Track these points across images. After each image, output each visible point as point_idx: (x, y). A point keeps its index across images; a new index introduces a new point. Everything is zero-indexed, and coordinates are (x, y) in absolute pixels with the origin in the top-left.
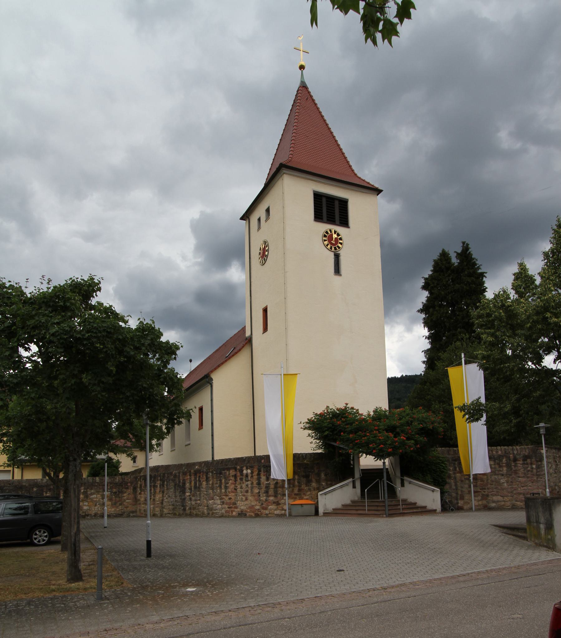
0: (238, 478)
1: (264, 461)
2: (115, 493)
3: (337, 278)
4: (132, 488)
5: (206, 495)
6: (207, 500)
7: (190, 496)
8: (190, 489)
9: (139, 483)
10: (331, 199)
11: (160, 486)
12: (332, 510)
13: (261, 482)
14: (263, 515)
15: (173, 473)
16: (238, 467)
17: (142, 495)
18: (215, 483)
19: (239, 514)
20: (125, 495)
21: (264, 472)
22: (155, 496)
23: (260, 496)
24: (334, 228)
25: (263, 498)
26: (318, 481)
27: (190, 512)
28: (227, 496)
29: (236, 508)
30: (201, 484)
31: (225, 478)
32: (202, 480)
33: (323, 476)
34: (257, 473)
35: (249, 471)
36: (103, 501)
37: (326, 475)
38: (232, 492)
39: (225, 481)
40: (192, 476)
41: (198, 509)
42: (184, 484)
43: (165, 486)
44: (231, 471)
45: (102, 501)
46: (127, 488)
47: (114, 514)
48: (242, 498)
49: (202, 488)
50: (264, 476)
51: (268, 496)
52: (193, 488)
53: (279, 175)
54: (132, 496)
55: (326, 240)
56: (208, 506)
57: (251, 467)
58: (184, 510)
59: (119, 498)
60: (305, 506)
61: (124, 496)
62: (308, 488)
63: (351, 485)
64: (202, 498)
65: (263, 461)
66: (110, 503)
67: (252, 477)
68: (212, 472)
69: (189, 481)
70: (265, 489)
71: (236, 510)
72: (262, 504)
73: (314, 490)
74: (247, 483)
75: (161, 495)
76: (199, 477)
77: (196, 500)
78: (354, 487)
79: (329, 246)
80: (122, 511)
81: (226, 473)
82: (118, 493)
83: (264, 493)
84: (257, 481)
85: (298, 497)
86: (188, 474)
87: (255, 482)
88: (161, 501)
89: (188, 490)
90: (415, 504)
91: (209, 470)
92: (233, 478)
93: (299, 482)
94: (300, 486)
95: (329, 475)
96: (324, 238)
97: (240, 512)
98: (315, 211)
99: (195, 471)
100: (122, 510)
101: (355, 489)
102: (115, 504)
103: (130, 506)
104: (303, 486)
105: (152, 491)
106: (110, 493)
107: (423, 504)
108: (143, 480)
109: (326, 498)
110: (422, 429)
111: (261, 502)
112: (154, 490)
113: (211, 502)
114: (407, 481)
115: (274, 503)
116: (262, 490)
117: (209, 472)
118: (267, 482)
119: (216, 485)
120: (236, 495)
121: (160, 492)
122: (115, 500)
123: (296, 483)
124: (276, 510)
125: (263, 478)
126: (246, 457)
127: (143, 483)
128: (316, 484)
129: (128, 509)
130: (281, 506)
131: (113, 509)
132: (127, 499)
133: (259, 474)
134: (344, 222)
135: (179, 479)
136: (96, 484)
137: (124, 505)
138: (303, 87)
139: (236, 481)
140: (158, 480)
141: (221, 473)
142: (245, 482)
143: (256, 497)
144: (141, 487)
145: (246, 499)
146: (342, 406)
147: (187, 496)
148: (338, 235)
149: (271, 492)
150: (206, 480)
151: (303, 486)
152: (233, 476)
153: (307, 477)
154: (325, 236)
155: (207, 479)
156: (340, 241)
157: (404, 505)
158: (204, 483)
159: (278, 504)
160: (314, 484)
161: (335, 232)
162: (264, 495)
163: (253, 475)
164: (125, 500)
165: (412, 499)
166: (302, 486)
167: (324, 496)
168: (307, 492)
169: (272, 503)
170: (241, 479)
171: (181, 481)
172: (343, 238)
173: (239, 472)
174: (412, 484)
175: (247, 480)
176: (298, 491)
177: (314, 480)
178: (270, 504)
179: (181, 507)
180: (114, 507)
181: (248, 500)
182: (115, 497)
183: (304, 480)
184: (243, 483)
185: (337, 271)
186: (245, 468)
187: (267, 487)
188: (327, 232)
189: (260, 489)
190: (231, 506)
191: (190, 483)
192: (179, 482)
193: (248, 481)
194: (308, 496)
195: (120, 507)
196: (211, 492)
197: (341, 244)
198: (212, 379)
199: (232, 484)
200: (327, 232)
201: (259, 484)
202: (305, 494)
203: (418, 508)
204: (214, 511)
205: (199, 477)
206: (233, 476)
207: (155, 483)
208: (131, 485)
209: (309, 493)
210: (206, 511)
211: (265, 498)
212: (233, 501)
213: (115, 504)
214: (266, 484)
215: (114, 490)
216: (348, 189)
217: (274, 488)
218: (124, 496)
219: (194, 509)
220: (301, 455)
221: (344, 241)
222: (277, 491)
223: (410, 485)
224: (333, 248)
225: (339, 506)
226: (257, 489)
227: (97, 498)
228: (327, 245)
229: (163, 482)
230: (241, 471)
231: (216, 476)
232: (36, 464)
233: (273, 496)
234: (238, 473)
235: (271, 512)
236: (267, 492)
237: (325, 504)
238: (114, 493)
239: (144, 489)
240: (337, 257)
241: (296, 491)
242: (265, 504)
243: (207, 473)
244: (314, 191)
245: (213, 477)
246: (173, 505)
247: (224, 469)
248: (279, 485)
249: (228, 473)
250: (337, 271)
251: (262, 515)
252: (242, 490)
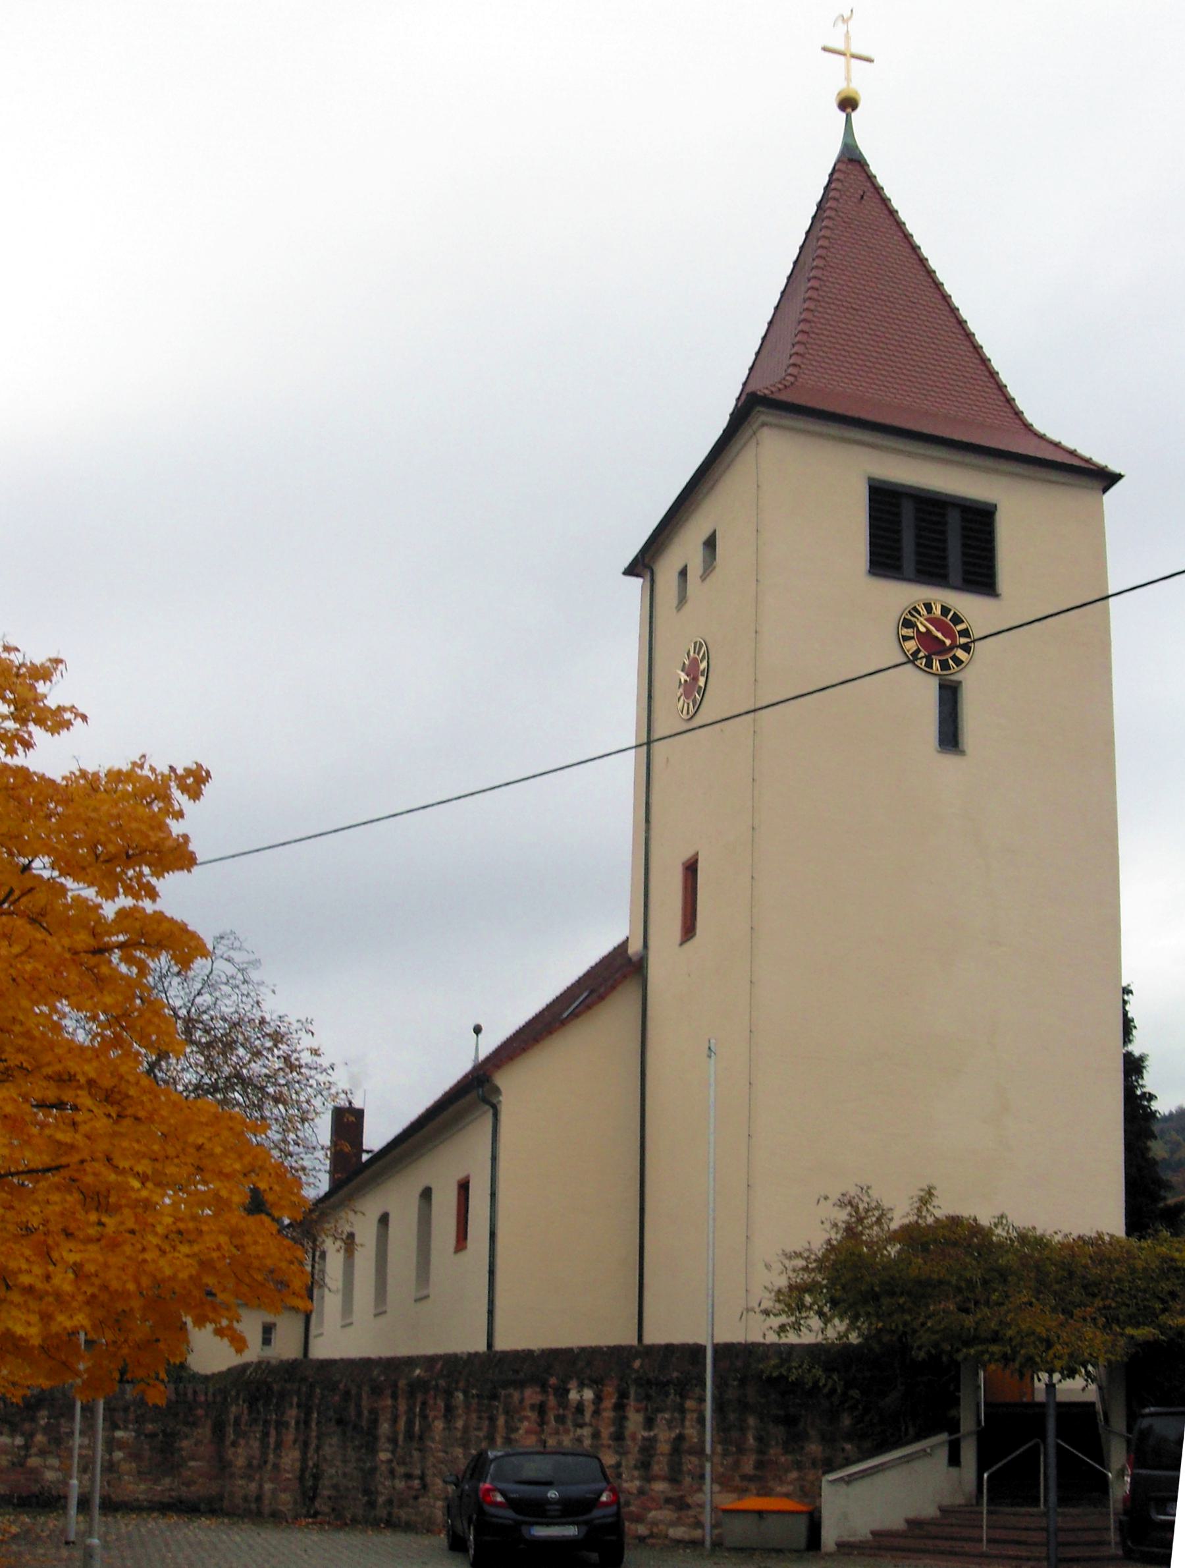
1: (642, 1366)
4: (209, 1422)
7: (390, 1461)
8: (393, 1440)
9: (234, 1409)
11: (297, 1423)
13: (627, 1433)
15: (341, 1386)
16: (553, 1380)
17: (240, 1450)
26: (828, 1439)
27: (390, 1514)
30: (427, 1428)
31: (507, 1413)
32: (431, 1414)
34: (613, 1401)
35: (588, 1394)
39: (506, 1422)
40: (400, 1399)
42: (374, 1422)
43: (313, 1426)
44: (528, 1392)
46: (194, 1424)
49: (433, 1440)
50: (638, 1411)
51: (649, 1479)
52: (401, 1438)
57: (596, 1383)
58: (371, 1504)
62: (790, 1457)
63: (943, 1454)
67: (597, 1412)
69: (389, 1416)
73: (814, 1464)
74: (579, 1431)
75: (296, 1454)
76: (424, 1404)
78: (954, 1460)
80: (173, 1494)
81: (510, 1396)
83: (636, 1467)
84: (612, 1429)
86: (388, 1392)
87: (606, 1432)
88: (298, 1474)
89: (383, 1443)
91: (457, 1382)
92: (533, 1415)
93: (759, 1439)
100: (171, 1490)
101: (957, 1469)
104: (774, 1452)
105: (272, 1440)
108: (244, 1401)
112: (278, 1433)
115: (668, 1501)
116: (630, 1456)
117: (457, 1389)
118: (646, 1434)
119: (477, 1433)
121: (295, 1441)
124: (673, 1524)
126: (583, 1350)
127: (246, 1412)
129: (193, 1489)
130: (691, 1513)
131: (143, 1487)
132: (193, 1459)
133: (620, 1407)
135: (358, 1406)
139: (542, 1422)
140: (291, 1405)
141: (494, 1397)
142: (572, 1429)
144: (239, 1425)
147: (382, 1462)
149: (660, 1466)
150: (445, 1416)
151: (774, 1452)
152: (532, 1407)
153: (789, 1421)
155: (449, 1412)
158: (439, 1425)
159: (680, 1504)
160: (814, 1448)
162: (636, 1473)
166: (772, 1451)
167: (843, 1489)
170: (561, 1419)
171: (366, 1413)
173: (555, 1394)
175: (580, 1421)
176: (756, 1468)
177: (812, 1433)
183: (779, 1432)
184: (567, 1431)
186: (573, 1384)
189: (622, 1452)
191: (394, 1420)
192: (359, 1414)
193: (581, 1426)
194: (791, 1483)
196: (461, 1456)
198: (497, 1091)
199: (528, 1432)
201: (619, 1437)
205: (424, 1404)
206: (532, 1407)
207: (283, 1414)
209: (794, 1475)
211: (637, 1483)
214: (644, 1439)
215: (150, 1427)
222: (680, 1464)
224: (936, 664)
225: (894, 1520)
229: (308, 1413)
233: (664, 1479)
234: (551, 1398)
235: (655, 1530)
236: (645, 1465)
238: (146, 1436)
239: (247, 1429)
240: (950, 695)
241: (748, 1466)
243: (449, 1394)
245: (468, 1407)
247: (506, 1384)
248: (686, 1446)
249: (516, 1395)
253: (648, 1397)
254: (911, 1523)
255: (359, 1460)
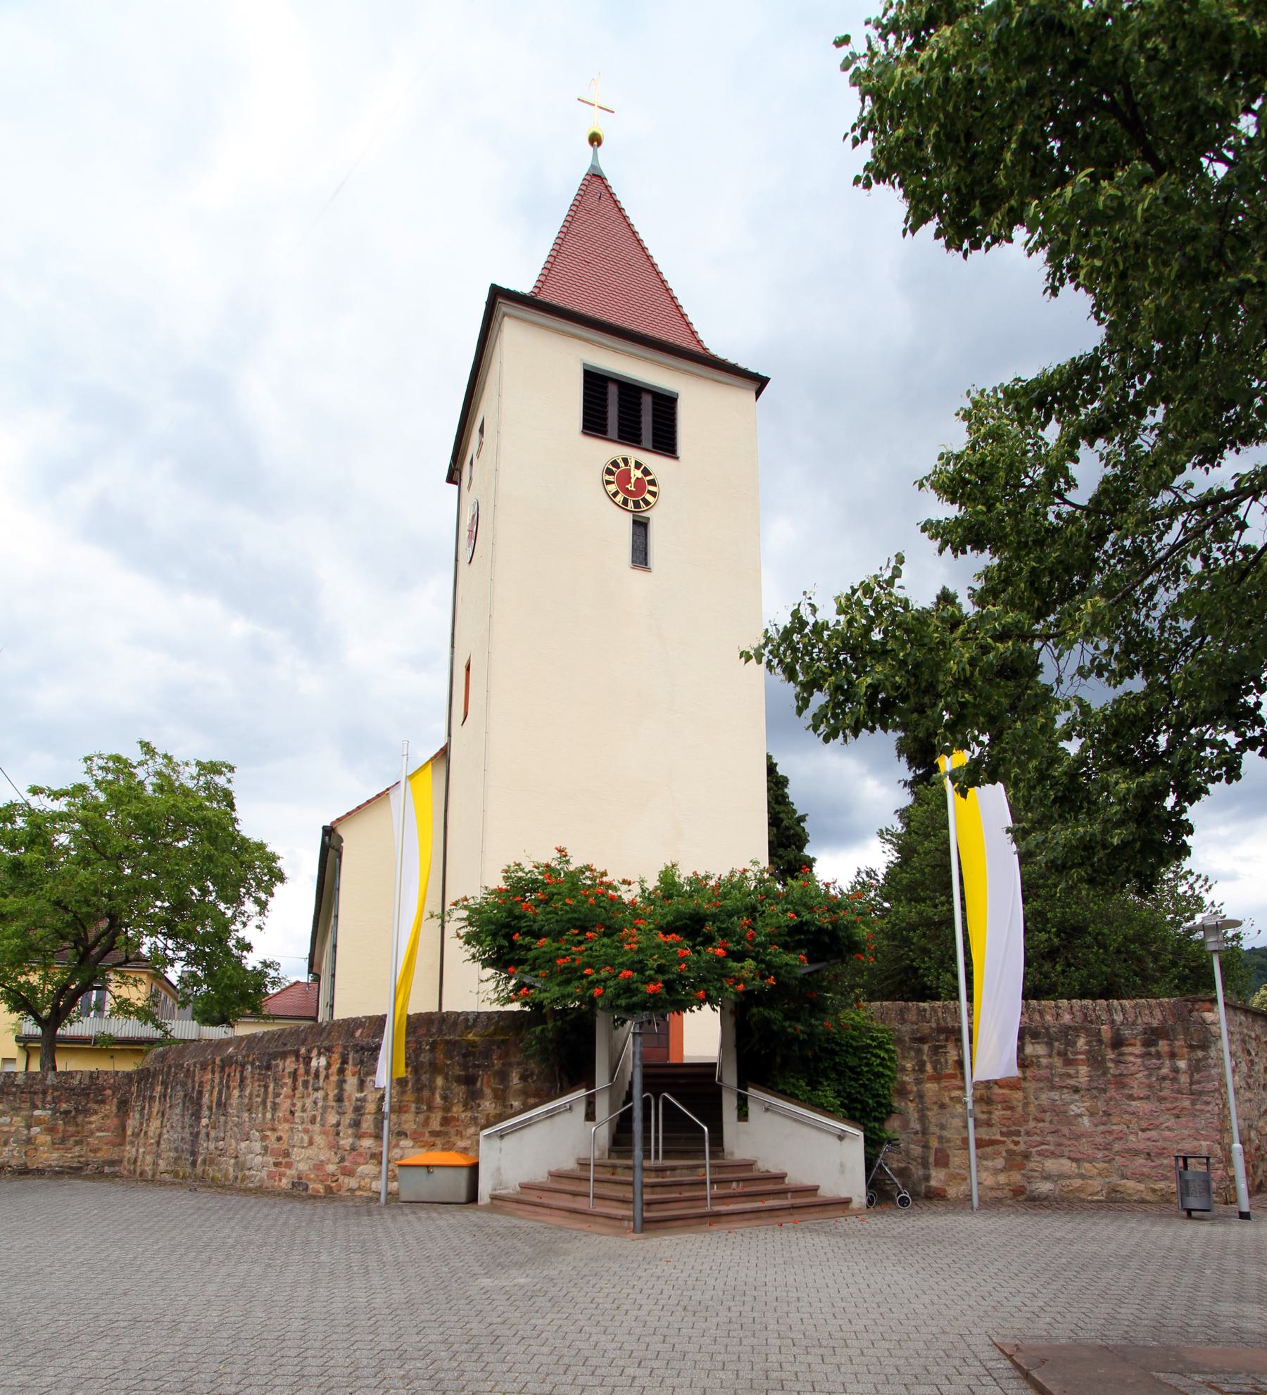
0: (300, 1080)
2: (67, 1113)
3: (639, 575)
4: (115, 1100)
5: (236, 1126)
6: (237, 1140)
8: (210, 1108)
10: (631, 391)
12: (518, 1189)
13: (346, 1095)
14: (344, 1193)
18: (255, 1093)
19: (293, 1184)
20: (93, 1118)
21: (355, 1065)
22: (148, 1125)
23: (338, 1134)
24: (633, 454)
25: (346, 1142)
26: (501, 1097)
28: (274, 1130)
29: (289, 1165)
30: (229, 1097)
31: (275, 1080)
32: (232, 1084)
33: (515, 1080)
35: (323, 1061)
36: (29, 1133)
37: (523, 1078)
38: (286, 1120)
41: (218, 1164)
45: (26, 1132)
46: (103, 1102)
47: (57, 1166)
48: (302, 1139)
49: (231, 1105)
51: (359, 1136)
53: (495, 326)
54: (112, 1122)
55: (613, 483)
56: (236, 1157)
58: (194, 1164)
59: (77, 1125)
60: (436, 1171)
61: (91, 1123)
62: (469, 1114)
63: (581, 1110)
64: (228, 1134)
65: (358, 1033)
66: (49, 1138)
67: (327, 1077)
68: (253, 1064)
70: (352, 1116)
71: (288, 1172)
72: (342, 1159)
75: (159, 1122)
76: (229, 1075)
77: (217, 1139)
78: (590, 1116)
79: (619, 498)
80: (82, 1159)
81: (277, 1066)
82: (73, 1113)
83: (350, 1126)
84: (336, 1091)
85: (439, 1141)
89: (205, 1112)
90: (781, 1177)
92: (288, 1081)
93: (445, 1098)
94: (447, 1109)
95: (535, 1077)
96: (608, 478)
97: (296, 1180)
98: (585, 413)
99: (222, 1060)
100: (80, 1156)
102: (63, 1140)
103: (105, 1147)
104: (457, 1110)
106: (50, 1112)
107: (808, 1181)
109: (501, 1150)
110: (800, 928)
111: (339, 1152)
113: (243, 1145)
114: (757, 1100)
118: (359, 1095)
120: (292, 1129)
122: (65, 1131)
123: (438, 1100)
125: (351, 1082)
128: (494, 1105)
129: (98, 1155)
131: (55, 1155)
132: (99, 1130)
133: (341, 1071)
134: (666, 443)
136: (14, 1090)
137: (88, 1144)
138: (596, 177)
139: (294, 1089)
141: (268, 1067)
143: (331, 1138)
145: (311, 1143)
146: (549, 856)
148: (646, 472)
149: (368, 1124)
150: (240, 1086)
151: (457, 1110)
153: (469, 1081)
154: (609, 472)
156: (652, 488)
157: (738, 1181)
158: (236, 1093)
160: (488, 1105)
161: (638, 465)
162: (350, 1131)
163: (330, 1071)
164: (92, 1133)
165: (769, 1162)
166: (455, 1109)
167: (496, 1143)
168: (466, 1127)
169: (368, 1156)
170: (306, 1083)
172: (658, 481)
174: (772, 1111)
176: (442, 1125)
177: (488, 1091)
178: (361, 1160)
179: (188, 1156)
180: (58, 1149)
181: (313, 1147)
182: (65, 1123)
183: (460, 1090)
185: (641, 556)
187: (359, 1110)
188: (615, 464)
190: (280, 1160)
194: (468, 1138)
195: (77, 1148)
197: (653, 494)
199: (286, 1097)
200: (615, 464)
201: (339, 1099)
202: (459, 1133)
203: (783, 1193)
204: (247, 1173)
205: (229, 1075)
208: (114, 1093)
210: (231, 1169)
211: (350, 1140)
212: (285, 1146)
213: (63, 1140)
214: (358, 1100)
215: (64, 1106)
216: (678, 369)
217: (376, 1113)
218: (91, 1123)
219: (212, 1162)
220: (462, 1018)
221: (662, 488)
223: (768, 1115)
224: (631, 504)
225: (538, 1174)
226: (334, 1112)
227: (11, 1124)
228: (615, 494)
229: (166, 1089)
230: (308, 1060)
231: (259, 1074)
232: (39, 1045)
235: (362, 1184)
236: (356, 1124)
237: (498, 1169)
238: (61, 1113)
240: (641, 526)
241: (435, 1125)
242: (350, 1158)
243: (243, 1066)
244: (584, 364)
246: (176, 1150)
247: (275, 1056)
250: (641, 556)
251: (339, 1190)
252: (305, 1115)
253: (362, 1062)
254: (556, 1176)
255: (191, 1126)
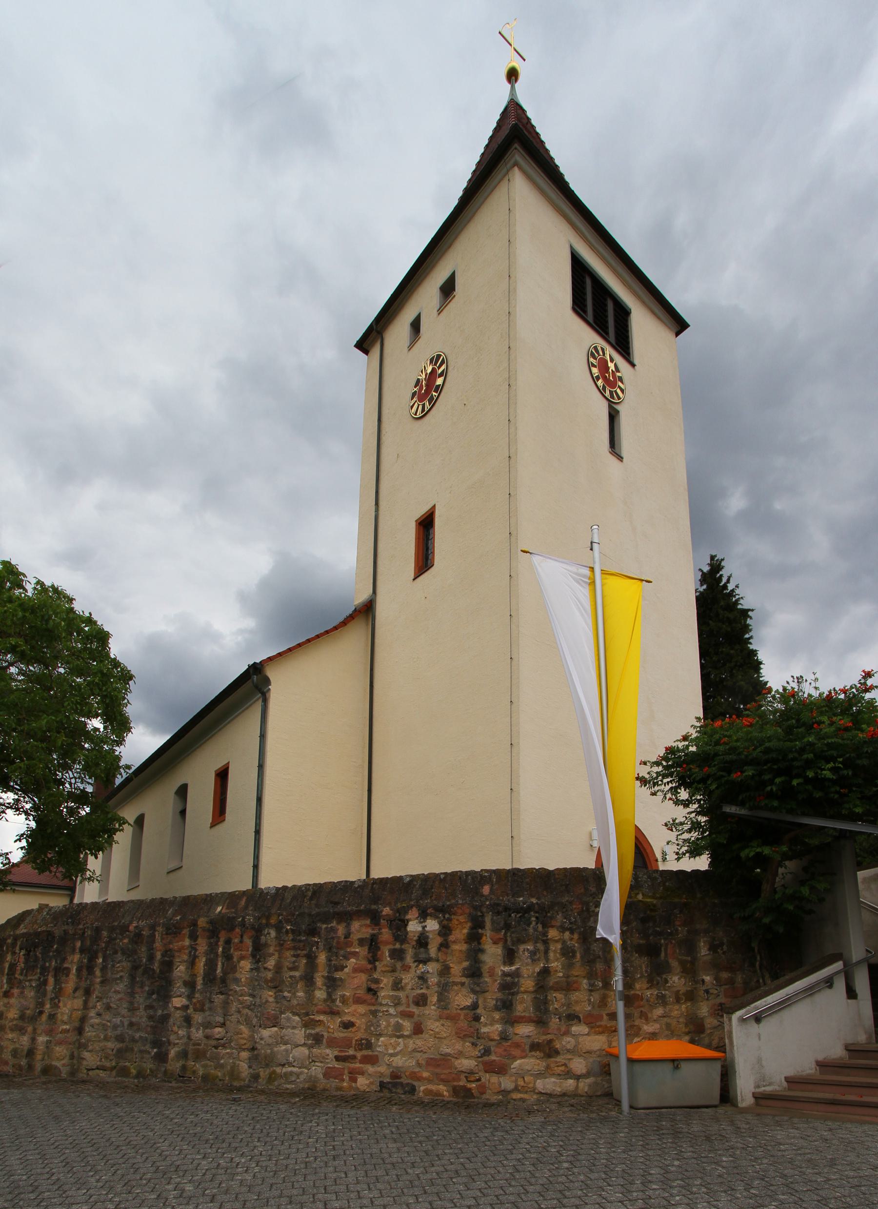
0: (385, 952)
1: (492, 891)
5: (248, 1007)
6: (252, 1027)
7: (185, 1008)
8: (190, 985)
9: (9, 957)
11: (79, 970)
12: (785, 1084)
13: (485, 969)
15: (131, 928)
16: (387, 911)
17: (13, 1001)
19: (382, 1085)
21: (496, 930)
22: (56, 1006)
23: (477, 1019)
25: (492, 1028)
27: (184, 1068)
28: (333, 1013)
29: (372, 1060)
30: (231, 968)
32: (236, 954)
34: (465, 931)
35: (432, 925)
38: (358, 1001)
39: (329, 960)
40: (200, 940)
42: (168, 965)
43: (98, 973)
44: (356, 925)
48: (398, 1027)
49: (237, 981)
50: (495, 943)
51: (511, 1021)
52: (200, 981)
56: (253, 1049)
57: (442, 911)
58: (161, 1057)
63: (840, 985)
64: (234, 1018)
65: (486, 890)
67: (444, 946)
68: (279, 928)
69: (185, 957)
70: (499, 995)
71: (371, 1069)
72: (487, 1052)
73: (678, 1000)
74: (422, 968)
75: (78, 1003)
76: (228, 942)
77: (207, 1025)
78: (851, 993)
81: (333, 930)
83: (497, 1008)
84: (466, 964)
86: (186, 931)
87: (457, 968)
88: (77, 1024)
89: (179, 988)
91: (268, 918)
92: (363, 951)
99: (211, 922)
101: (854, 1001)
104: (640, 987)
105: (50, 987)
108: (21, 949)
112: (57, 981)
113: (266, 1033)
115: (534, 1047)
116: (488, 995)
117: (268, 925)
118: (507, 969)
119: (292, 973)
120: (374, 1013)
121: (76, 990)
124: (540, 1075)
126: (414, 878)
127: (22, 959)
130: (559, 1059)
133: (474, 938)
135: (151, 948)
140: (73, 951)
142: (413, 965)
143: (463, 1024)
144: (14, 974)
145: (418, 1030)
147: (176, 1008)
149: (524, 1005)
150: (253, 956)
151: (640, 987)
152: (361, 942)
155: (258, 952)
158: (246, 965)
159: (548, 1050)
162: (497, 1016)
163: (452, 938)
166: (637, 986)
167: (754, 1027)
168: (652, 1007)
169: (527, 1047)
170: (397, 955)
171: (158, 955)
173: (390, 929)
175: (423, 956)
177: (674, 964)
178: (516, 1052)
179: (148, 1047)
183: (642, 963)
184: (406, 968)
186: (413, 914)
189: (478, 991)
190: (351, 1052)
191: (192, 963)
192: (151, 958)
193: (425, 962)
196: (271, 999)
199: (355, 970)
201: (474, 973)
202: (644, 1016)
204: (278, 1070)
205: (228, 942)
206: (361, 942)
207: (64, 960)
209: (659, 1011)
210: (244, 1066)
211: (499, 1027)
212: (360, 1035)
214: (505, 974)
217: (536, 992)
219: (199, 1055)
222: (546, 1002)
226: (464, 991)
229: (92, 959)
230: (399, 925)
233: (529, 1020)
234: (385, 931)
236: (506, 1006)
239: (22, 978)
242: (500, 1051)
243: (258, 931)
245: (281, 945)
246: (120, 1038)
247: (326, 918)
248: (552, 981)
249: (341, 930)
251: (482, 1093)
252: (401, 994)
253: (507, 927)
254: (822, 1065)
255: (149, 1007)
